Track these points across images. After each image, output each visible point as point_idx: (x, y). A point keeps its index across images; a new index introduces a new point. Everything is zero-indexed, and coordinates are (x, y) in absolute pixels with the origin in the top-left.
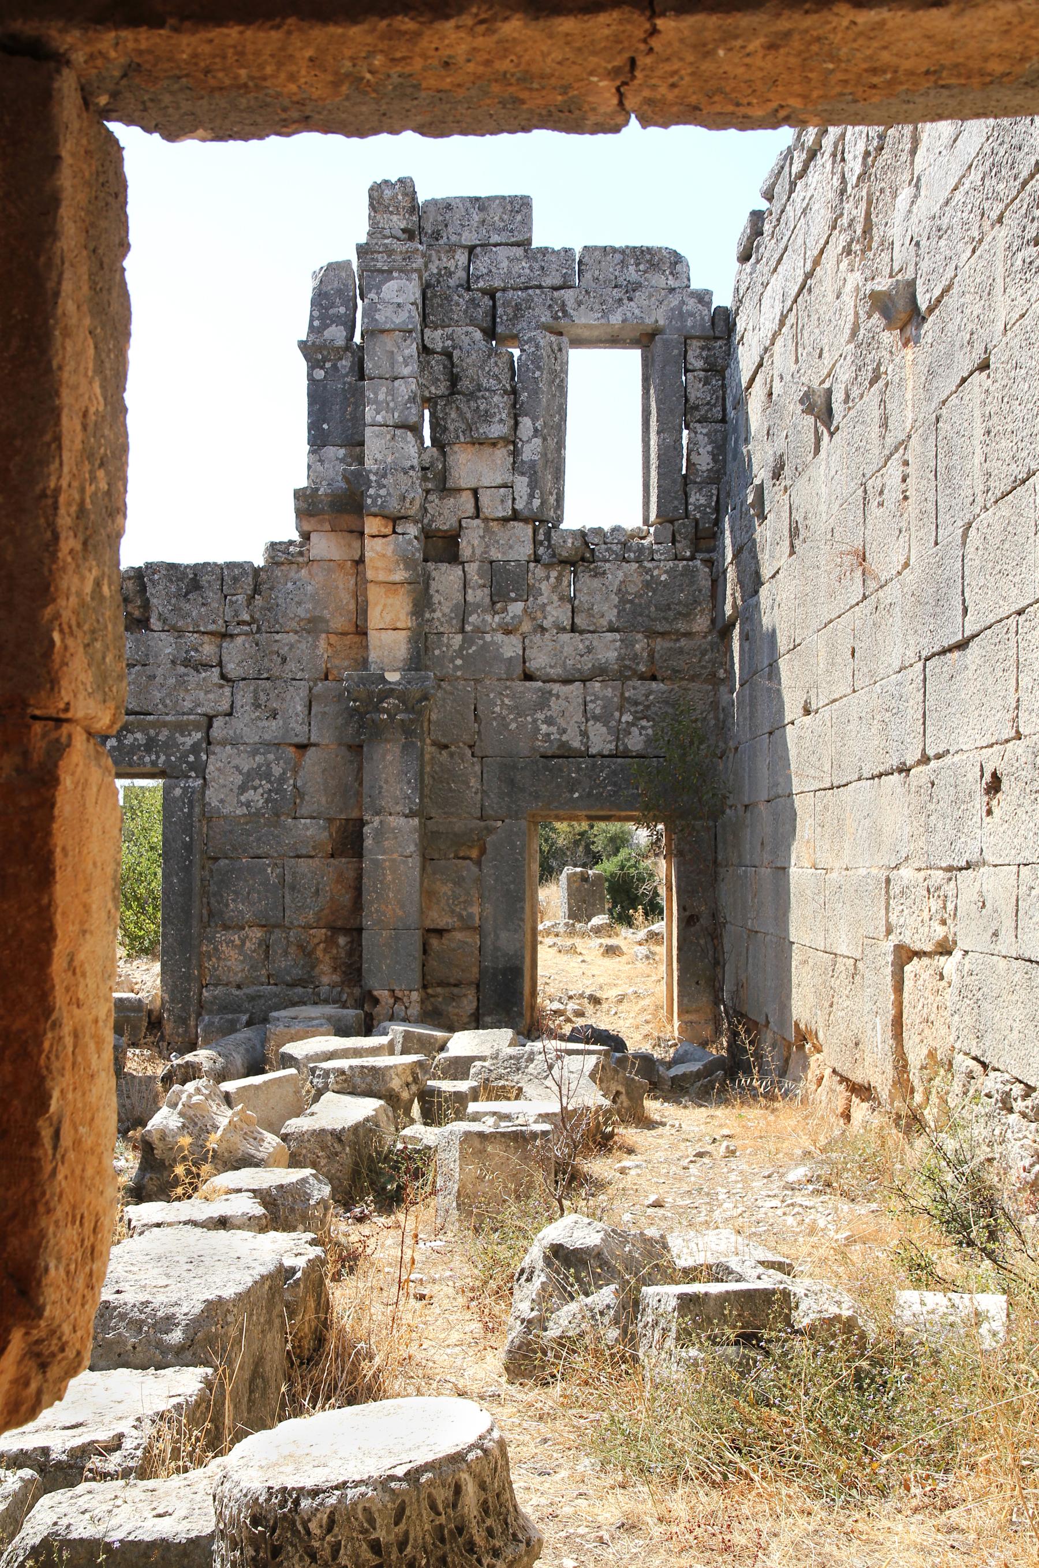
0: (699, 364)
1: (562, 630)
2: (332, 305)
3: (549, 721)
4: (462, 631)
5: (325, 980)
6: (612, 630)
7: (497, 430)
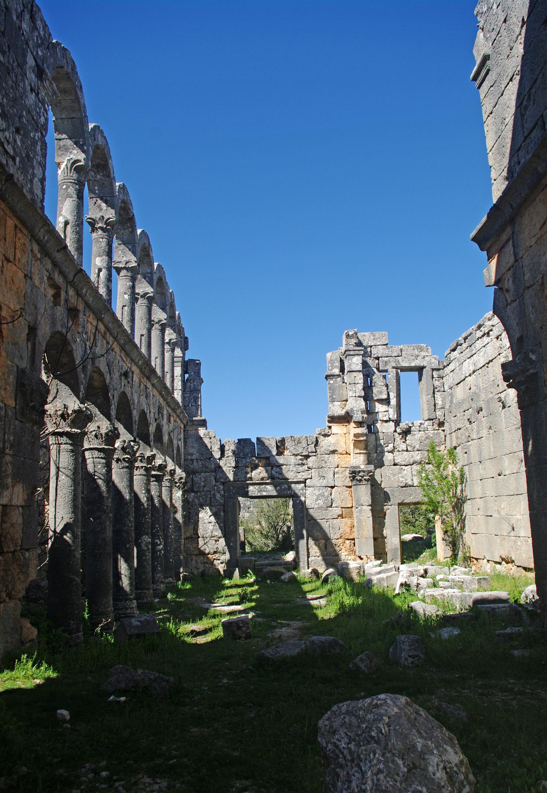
3: (402, 477)
4: (376, 452)
6: (418, 450)
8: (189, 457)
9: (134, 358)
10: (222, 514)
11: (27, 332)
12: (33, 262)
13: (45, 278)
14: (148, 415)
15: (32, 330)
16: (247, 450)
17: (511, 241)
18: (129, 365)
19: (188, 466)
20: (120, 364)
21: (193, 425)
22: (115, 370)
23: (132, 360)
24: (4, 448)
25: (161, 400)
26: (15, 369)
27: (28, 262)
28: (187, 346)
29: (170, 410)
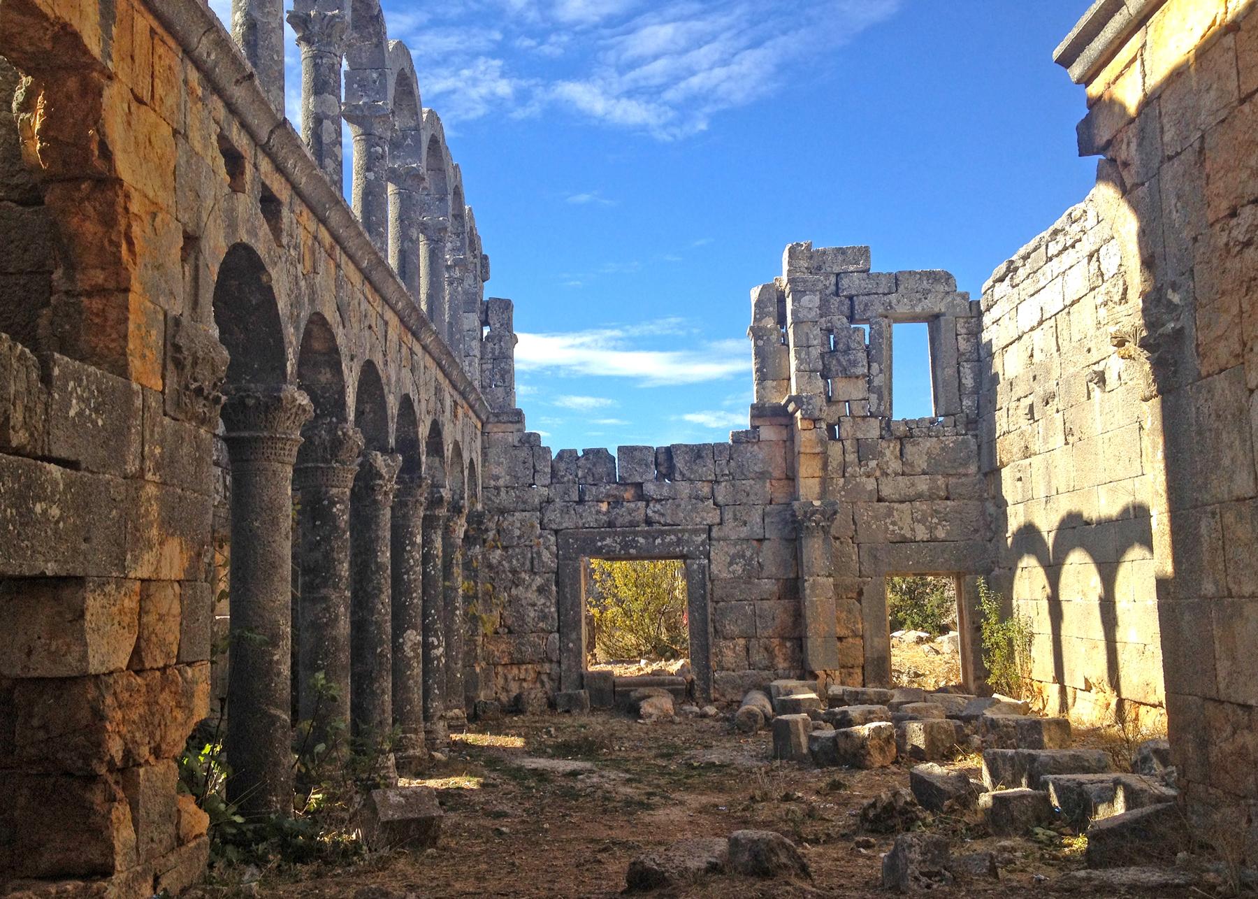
0: (963, 331)
1: (897, 474)
2: (766, 307)
3: (894, 523)
5: (780, 666)
7: (861, 370)
8: (492, 483)
9: (388, 296)
10: (554, 588)
11: (181, 244)
12: (189, 105)
13: (214, 137)
14: (416, 404)
15: (191, 241)
16: (601, 470)
17: (1138, 62)
18: (379, 309)
19: (490, 499)
20: (362, 307)
21: (499, 422)
22: (353, 320)
23: (385, 300)
24: (142, 469)
25: (440, 376)
26: (161, 317)
27: (178, 105)
28: (487, 272)
29: (455, 394)
